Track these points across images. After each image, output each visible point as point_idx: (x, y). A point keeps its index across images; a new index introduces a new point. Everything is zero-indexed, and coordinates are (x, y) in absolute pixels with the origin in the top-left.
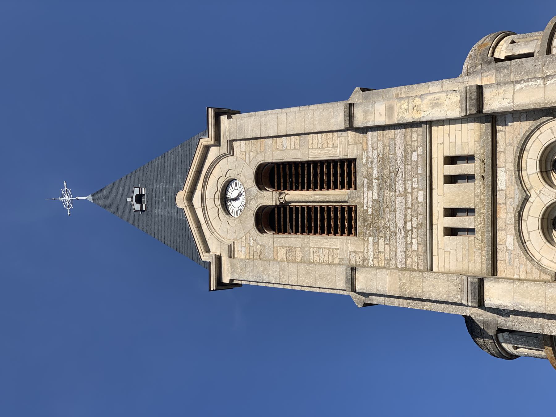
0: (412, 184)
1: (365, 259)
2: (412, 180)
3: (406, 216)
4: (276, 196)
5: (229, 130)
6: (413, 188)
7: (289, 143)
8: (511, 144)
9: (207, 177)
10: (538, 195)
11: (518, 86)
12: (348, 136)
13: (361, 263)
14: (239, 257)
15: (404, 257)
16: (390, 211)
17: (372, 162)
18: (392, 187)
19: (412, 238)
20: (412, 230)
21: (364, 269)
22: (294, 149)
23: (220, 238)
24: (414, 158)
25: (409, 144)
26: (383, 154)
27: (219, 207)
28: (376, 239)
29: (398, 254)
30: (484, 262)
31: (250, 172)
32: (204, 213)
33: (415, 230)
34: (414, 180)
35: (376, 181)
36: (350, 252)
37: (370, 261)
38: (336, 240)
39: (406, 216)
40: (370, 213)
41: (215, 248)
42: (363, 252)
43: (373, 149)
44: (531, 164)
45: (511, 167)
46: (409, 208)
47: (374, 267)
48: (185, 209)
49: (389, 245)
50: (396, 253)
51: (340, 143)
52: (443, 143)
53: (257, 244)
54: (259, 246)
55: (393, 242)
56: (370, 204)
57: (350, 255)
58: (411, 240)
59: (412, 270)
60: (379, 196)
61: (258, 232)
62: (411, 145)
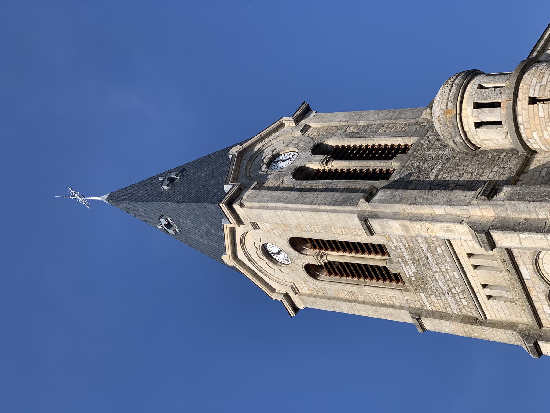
4: (318, 259)
18: (427, 265)
19: (460, 299)
30: (529, 315)
32: (254, 264)
33: (461, 294)
39: (448, 285)
41: (280, 289)
55: (443, 298)
56: (412, 275)
62: (433, 244)
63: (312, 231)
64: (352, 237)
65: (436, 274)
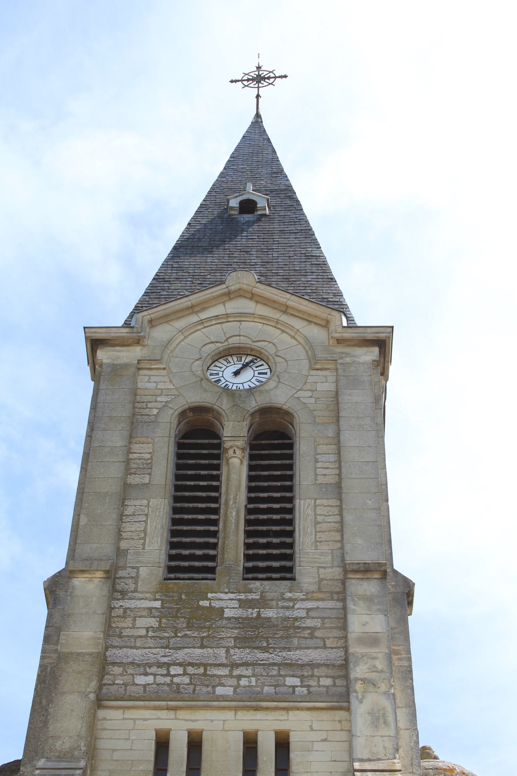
0: (245, 677)
1: (124, 593)
2: (253, 675)
5: (354, 362)
6: (239, 677)
7: (326, 465)
12: (332, 567)
13: (118, 587)
14: (140, 378)
15: (124, 661)
16: (203, 638)
17: (288, 608)
18: (243, 642)
19: (155, 675)
20: (168, 674)
21: (105, 592)
22: (316, 475)
23: (174, 345)
24: (290, 681)
25: (313, 672)
26: (299, 628)
27: (226, 343)
29: (130, 651)
31: (280, 397)
33: (168, 680)
34: (253, 679)
35: (255, 615)
36: (137, 568)
37: (121, 603)
38: (159, 544)
40: (201, 603)
42: (136, 591)
43: (309, 610)
46: (205, 670)
47: (111, 609)
48: (224, 286)
49: (146, 636)
50: (131, 648)
51: (322, 554)
52: (312, 729)
53: (160, 409)
54: (155, 412)
55: (151, 643)
56: (216, 604)
57: (133, 568)
58: (151, 674)
59: (102, 673)
60: (229, 619)
61: (180, 410)
62: (312, 676)
63: (317, 461)
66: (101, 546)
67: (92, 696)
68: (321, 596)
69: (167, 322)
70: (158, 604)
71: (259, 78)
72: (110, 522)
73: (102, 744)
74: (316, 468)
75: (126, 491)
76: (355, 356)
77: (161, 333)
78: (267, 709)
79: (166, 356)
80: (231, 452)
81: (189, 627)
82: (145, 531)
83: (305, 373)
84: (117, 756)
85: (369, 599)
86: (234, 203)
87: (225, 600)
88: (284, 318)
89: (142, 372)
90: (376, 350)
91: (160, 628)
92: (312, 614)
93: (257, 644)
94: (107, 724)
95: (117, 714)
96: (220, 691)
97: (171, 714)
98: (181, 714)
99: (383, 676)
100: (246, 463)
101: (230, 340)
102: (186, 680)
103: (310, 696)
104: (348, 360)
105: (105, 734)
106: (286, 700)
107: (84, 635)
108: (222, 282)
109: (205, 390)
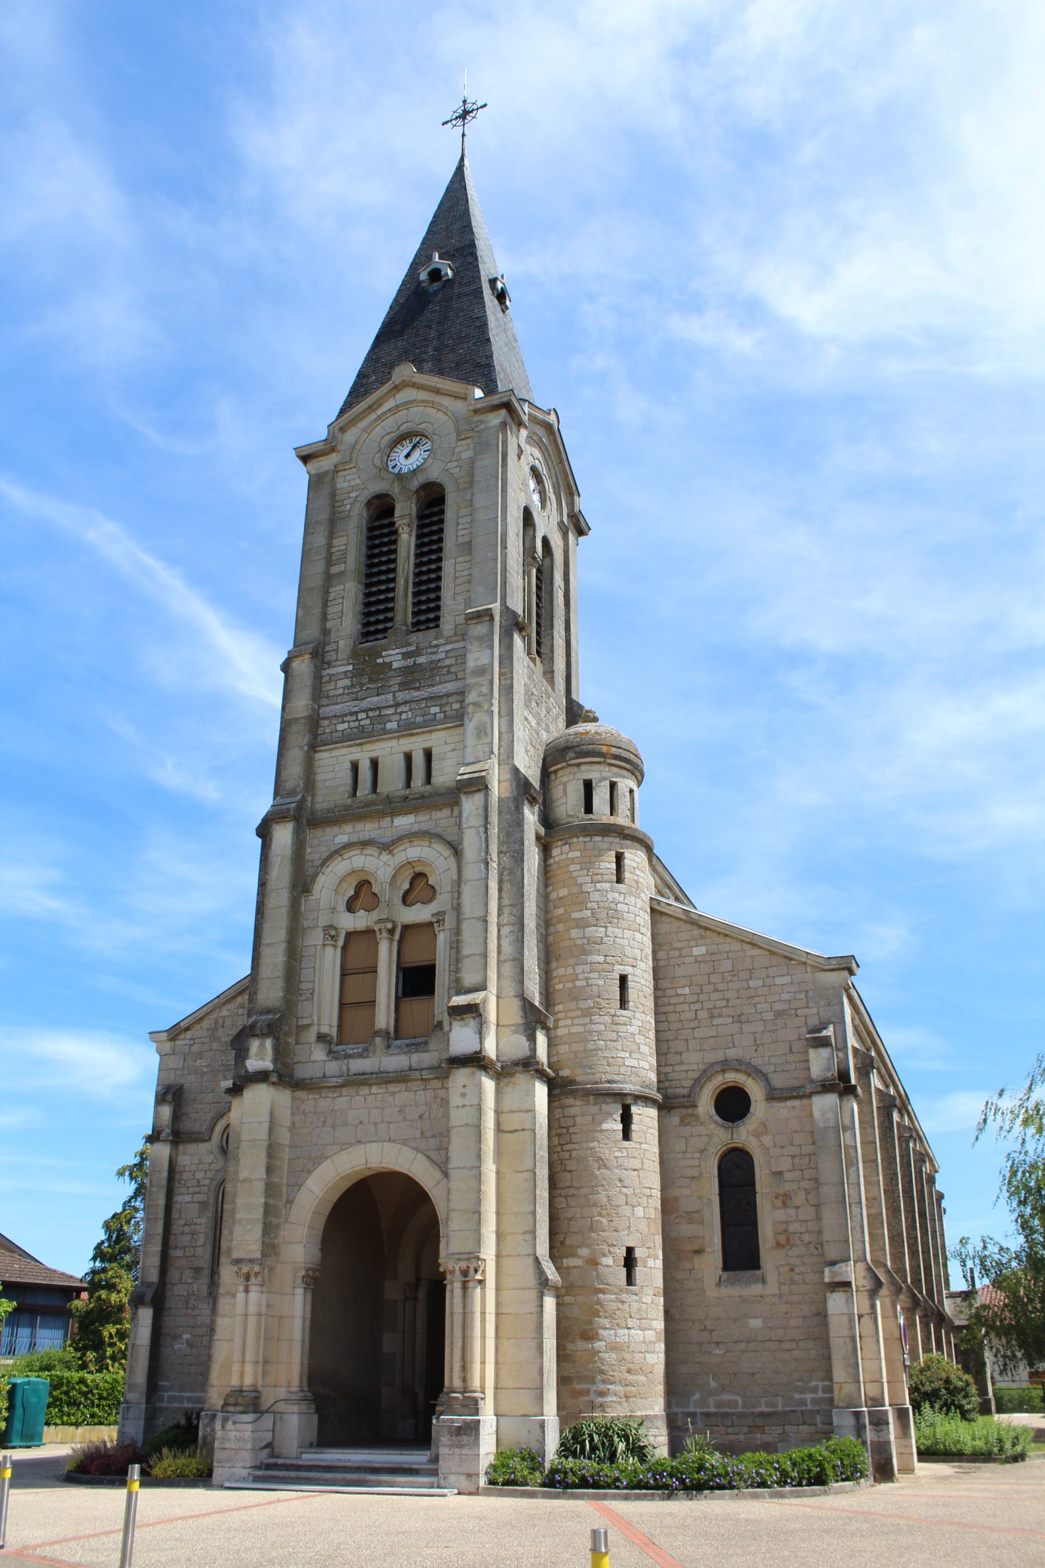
2: (410, 710)
3: (371, 709)
6: (401, 713)
8: (437, 825)
9: (433, 405)
10: (385, 864)
11: (482, 829)
17: (434, 653)
18: (405, 686)
20: (357, 720)
24: (434, 710)
28: (349, 675)
31: (434, 474)
33: (357, 724)
37: (328, 671)
39: (371, 709)
42: (337, 660)
43: (447, 652)
44: (414, 852)
45: (415, 828)
49: (342, 694)
54: (348, 507)
55: (346, 698)
56: (387, 660)
63: (458, 524)
64: (452, 585)
65: (390, 696)
66: (313, 632)
67: (306, 748)
68: (456, 638)
69: (354, 425)
70: (350, 668)
71: (464, 115)
72: (317, 611)
73: (320, 777)
74: (457, 530)
75: (329, 579)
76: (486, 422)
77: (350, 436)
78: (417, 734)
79: (355, 456)
80: (400, 529)
81: (371, 681)
82: (342, 611)
83: (453, 445)
84: (327, 784)
85: (480, 639)
86: (423, 276)
87: (394, 657)
88: (438, 399)
89: (340, 474)
90: (503, 412)
91: (353, 686)
92: (449, 655)
93: (413, 685)
94: (321, 763)
95: (326, 755)
96: (389, 726)
97: (359, 748)
98: (366, 747)
99: (486, 698)
100: (414, 534)
101: (401, 428)
102: (368, 722)
103: (447, 719)
104: (482, 427)
105: (320, 770)
106: (429, 724)
107: (302, 704)
108: (389, 380)
109: (383, 479)
